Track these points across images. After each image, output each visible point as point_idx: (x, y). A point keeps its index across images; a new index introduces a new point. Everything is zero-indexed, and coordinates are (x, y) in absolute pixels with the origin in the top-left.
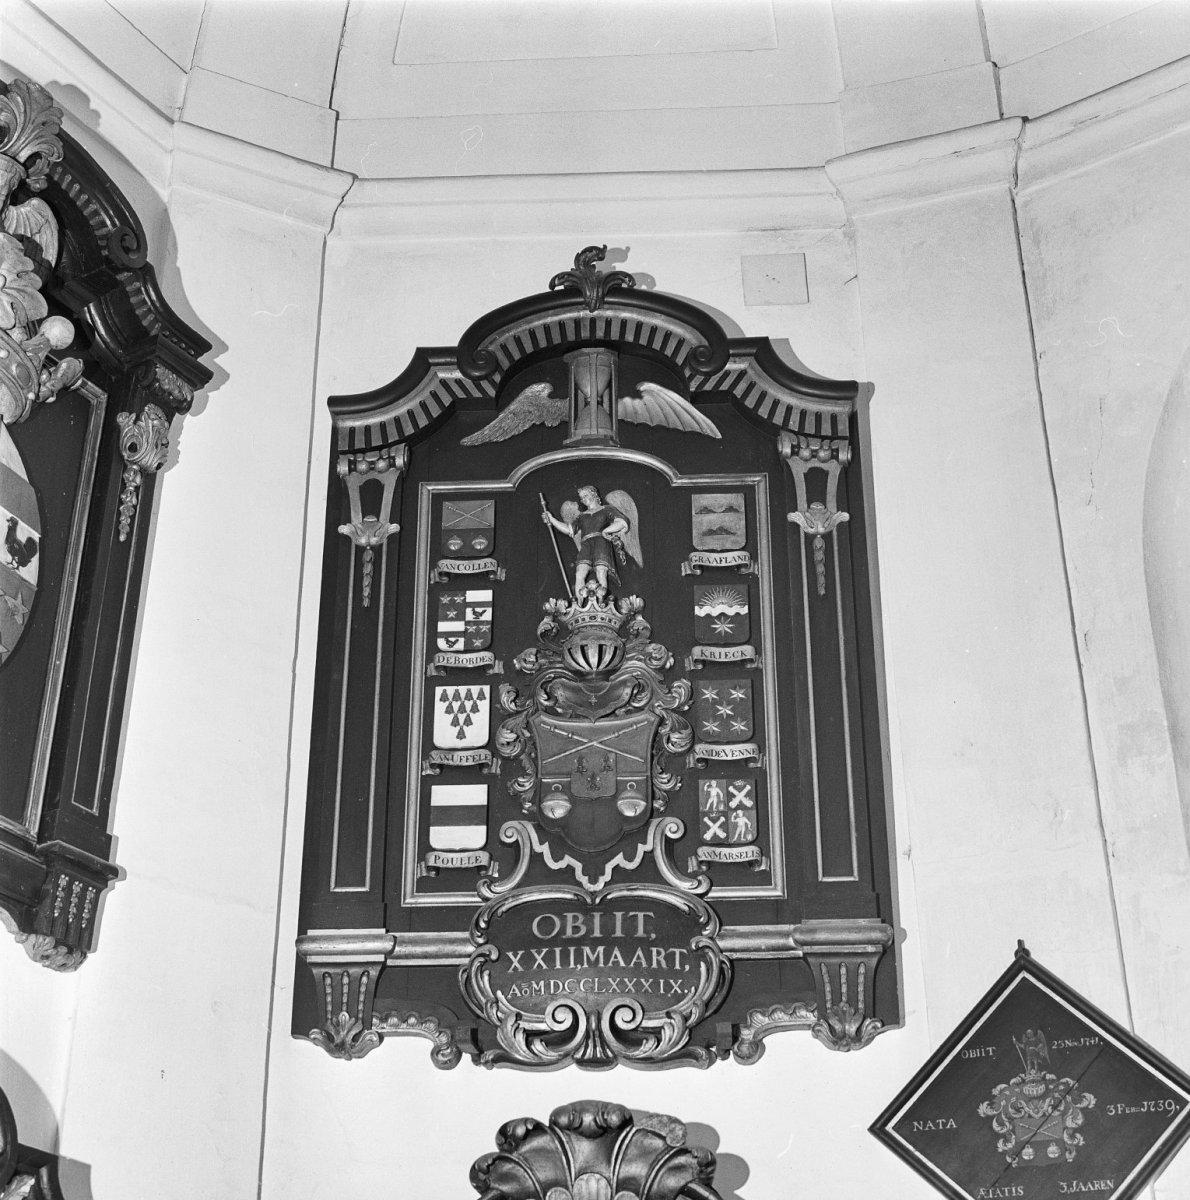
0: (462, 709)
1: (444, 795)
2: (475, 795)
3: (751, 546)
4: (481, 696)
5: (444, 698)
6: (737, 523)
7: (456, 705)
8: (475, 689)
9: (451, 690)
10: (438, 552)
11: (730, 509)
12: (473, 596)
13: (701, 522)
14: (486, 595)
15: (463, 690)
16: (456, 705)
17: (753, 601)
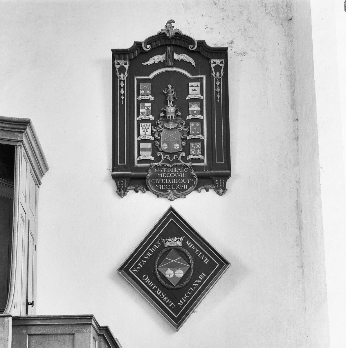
0: (145, 129)
1: (142, 145)
2: (149, 145)
3: (201, 93)
4: (149, 126)
5: (143, 129)
6: (198, 89)
7: (144, 128)
8: (148, 124)
9: (143, 124)
10: (139, 94)
11: (197, 86)
12: (147, 104)
13: (191, 89)
14: (149, 104)
15: (145, 124)
16: (144, 128)
17: (202, 107)
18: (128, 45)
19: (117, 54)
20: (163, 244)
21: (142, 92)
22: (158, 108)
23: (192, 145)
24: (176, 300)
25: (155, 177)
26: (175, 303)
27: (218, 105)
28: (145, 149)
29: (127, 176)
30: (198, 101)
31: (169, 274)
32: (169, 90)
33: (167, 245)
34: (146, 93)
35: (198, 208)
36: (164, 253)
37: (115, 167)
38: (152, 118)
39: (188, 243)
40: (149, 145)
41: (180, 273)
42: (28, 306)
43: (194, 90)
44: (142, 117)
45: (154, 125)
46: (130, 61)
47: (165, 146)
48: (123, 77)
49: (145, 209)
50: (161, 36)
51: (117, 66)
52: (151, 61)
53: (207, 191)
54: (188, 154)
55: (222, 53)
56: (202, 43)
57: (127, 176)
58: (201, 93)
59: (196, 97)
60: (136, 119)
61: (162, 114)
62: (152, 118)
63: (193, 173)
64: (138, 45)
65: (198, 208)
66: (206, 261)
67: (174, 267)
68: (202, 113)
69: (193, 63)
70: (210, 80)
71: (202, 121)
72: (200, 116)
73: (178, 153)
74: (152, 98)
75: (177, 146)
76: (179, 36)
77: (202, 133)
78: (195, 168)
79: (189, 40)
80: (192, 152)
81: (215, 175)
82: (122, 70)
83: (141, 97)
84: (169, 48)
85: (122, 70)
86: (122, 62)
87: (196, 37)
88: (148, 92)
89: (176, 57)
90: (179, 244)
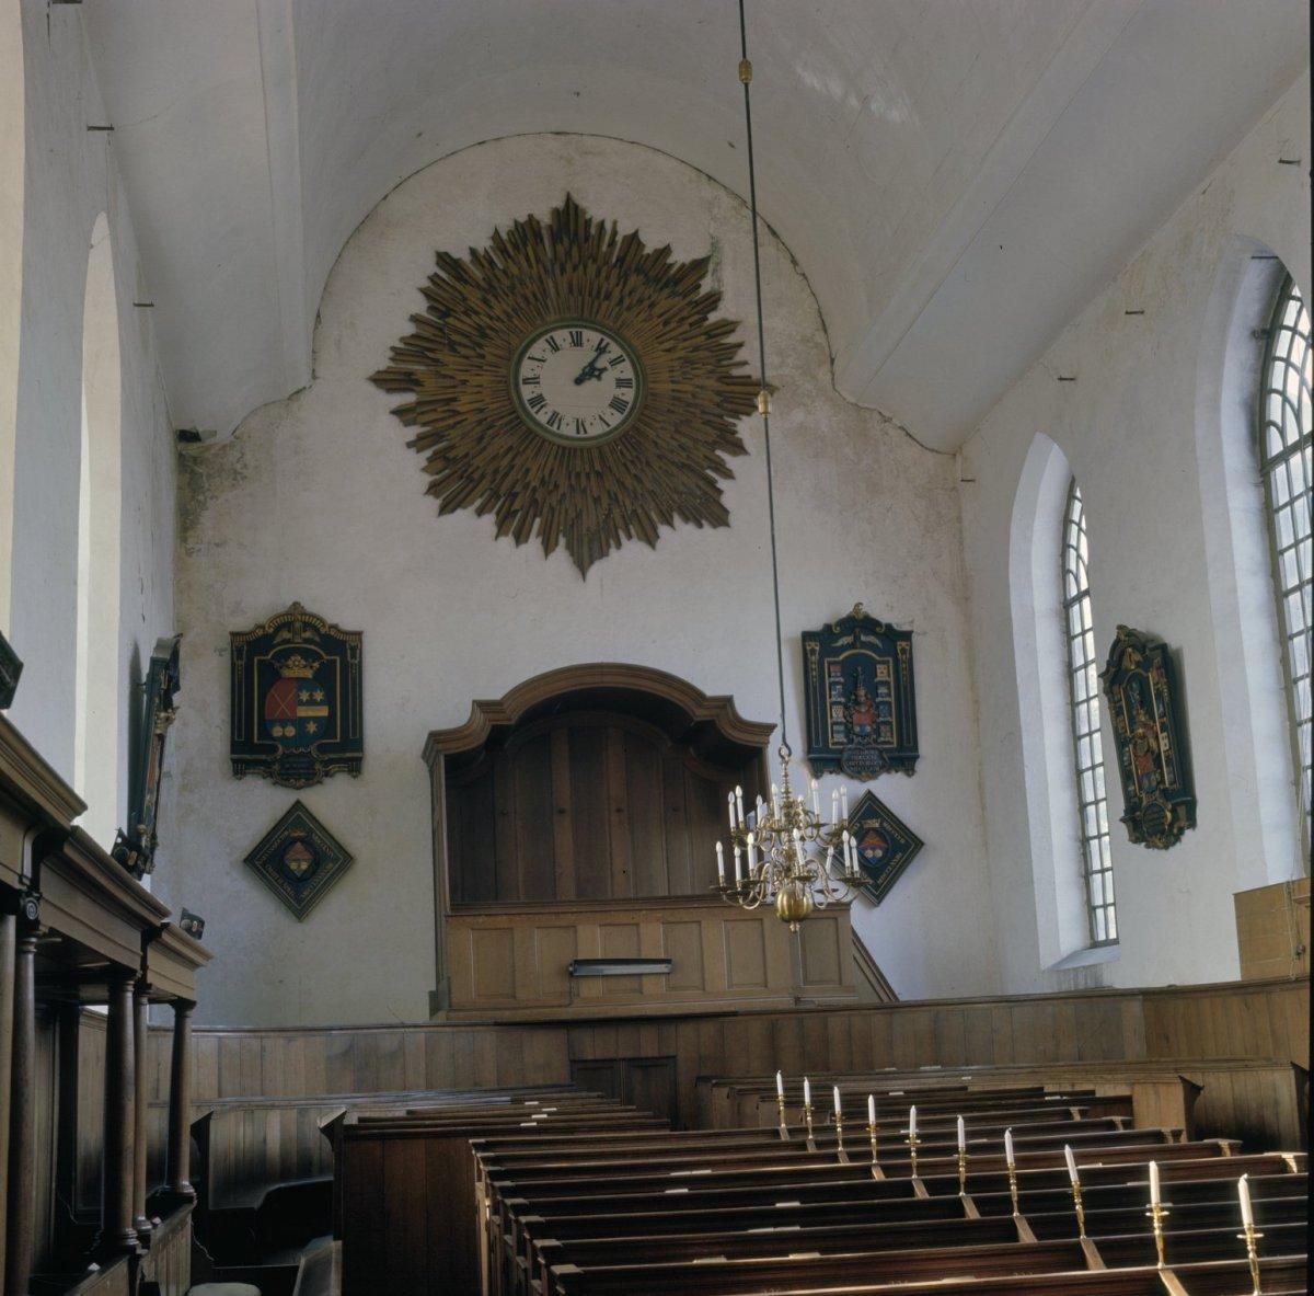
1: (835, 728)
3: (889, 676)
6: (885, 671)
10: (830, 676)
13: (878, 671)
19: (807, 636)
20: (862, 826)
21: (833, 674)
22: (850, 691)
23: (882, 728)
24: (875, 878)
25: (849, 760)
26: (877, 879)
27: (905, 688)
28: (838, 732)
30: (886, 684)
33: (867, 826)
38: (843, 700)
39: (885, 824)
40: (842, 728)
41: (879, 853)
42: (200, 943)
43: (883, 673)
44: (834, 699)
45: (846, 707)
46: (820, 647)
47: (857, 729)
51: (808, 648)
52: (840, 643)
53: (897, 771)
54: (879, 735)
55: (907, 636)
56: (889, 626)
58: (889, 676)
59: (884, 679)
60: (828, 701)
61: (853, 697)
62: (843, 700)
63: (885, 756)
64: (828, 627)
65: (890, 788)
66: (903, 841)
68: (889, 695)
69: (880, 645)
70: (896, 662)
71: (890, 703)
72: (887, 699)
73: (868, 735)
74: (842, 680)
75: (868, 729)
77: (891, 715)
78: (887, 750)
79: (877, 623)
80: (883, 734)
81: (903, 758)
82: (813, 651)
83: (832, 679)
84: (857, 630)
86: (813, 644)
88: (839, 674)
89: (863, 638)
90: (877, 825)
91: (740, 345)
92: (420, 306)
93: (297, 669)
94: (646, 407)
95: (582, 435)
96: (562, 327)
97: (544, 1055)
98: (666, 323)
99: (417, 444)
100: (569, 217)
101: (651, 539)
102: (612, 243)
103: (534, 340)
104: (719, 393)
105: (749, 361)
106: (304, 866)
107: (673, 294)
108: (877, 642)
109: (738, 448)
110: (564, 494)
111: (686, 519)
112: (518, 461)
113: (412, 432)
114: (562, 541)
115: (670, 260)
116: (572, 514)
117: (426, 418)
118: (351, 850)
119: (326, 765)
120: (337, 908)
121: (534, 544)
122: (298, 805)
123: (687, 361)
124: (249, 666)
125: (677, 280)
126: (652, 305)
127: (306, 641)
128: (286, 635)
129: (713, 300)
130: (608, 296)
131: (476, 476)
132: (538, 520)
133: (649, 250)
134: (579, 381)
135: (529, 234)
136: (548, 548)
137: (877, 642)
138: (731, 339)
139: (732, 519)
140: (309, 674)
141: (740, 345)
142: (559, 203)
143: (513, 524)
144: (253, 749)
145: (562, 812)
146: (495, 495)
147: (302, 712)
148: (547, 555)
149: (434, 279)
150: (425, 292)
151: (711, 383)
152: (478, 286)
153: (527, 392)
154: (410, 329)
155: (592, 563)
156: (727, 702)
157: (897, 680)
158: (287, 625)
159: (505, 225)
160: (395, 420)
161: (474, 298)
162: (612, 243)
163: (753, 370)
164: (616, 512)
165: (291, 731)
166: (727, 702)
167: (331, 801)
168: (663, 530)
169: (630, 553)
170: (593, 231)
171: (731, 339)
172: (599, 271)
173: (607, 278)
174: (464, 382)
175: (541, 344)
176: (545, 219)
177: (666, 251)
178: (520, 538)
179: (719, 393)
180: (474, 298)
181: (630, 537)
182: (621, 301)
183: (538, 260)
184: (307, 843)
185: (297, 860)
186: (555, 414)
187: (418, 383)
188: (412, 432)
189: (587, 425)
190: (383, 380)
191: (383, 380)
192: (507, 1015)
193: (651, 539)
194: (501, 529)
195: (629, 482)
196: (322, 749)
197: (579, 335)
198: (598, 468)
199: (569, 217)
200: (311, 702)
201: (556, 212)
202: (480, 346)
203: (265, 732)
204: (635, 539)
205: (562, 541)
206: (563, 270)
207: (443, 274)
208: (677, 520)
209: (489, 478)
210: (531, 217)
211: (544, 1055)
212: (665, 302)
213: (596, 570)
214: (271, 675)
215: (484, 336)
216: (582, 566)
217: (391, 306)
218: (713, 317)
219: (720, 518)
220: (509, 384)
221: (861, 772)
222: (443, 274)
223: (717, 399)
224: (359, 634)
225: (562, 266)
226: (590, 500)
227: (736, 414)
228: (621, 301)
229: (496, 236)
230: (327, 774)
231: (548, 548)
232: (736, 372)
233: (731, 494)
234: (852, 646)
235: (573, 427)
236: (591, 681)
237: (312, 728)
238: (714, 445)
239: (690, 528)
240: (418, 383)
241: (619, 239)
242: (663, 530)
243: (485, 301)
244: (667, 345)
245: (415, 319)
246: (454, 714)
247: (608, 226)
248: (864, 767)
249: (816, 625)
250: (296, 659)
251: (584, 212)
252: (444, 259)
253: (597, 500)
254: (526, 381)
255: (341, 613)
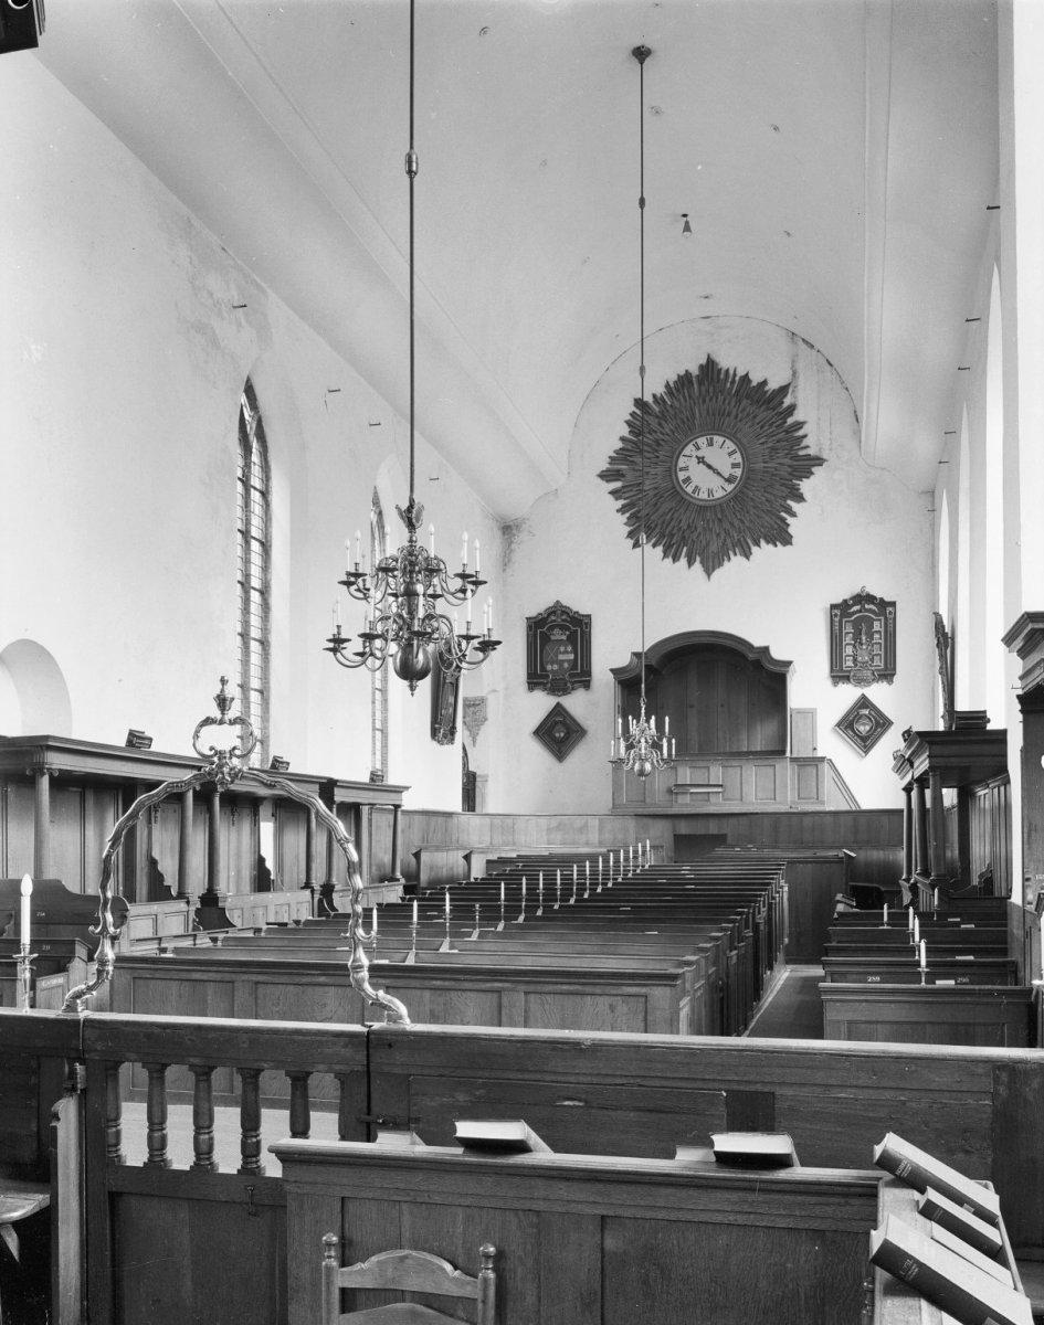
18: (839, 601)
19: (833, 607)
29: (839, 675)
31: (862, 728)
32: (862, 628)
34: (849, 628)
35: (878, 693)
36: (859, 717)
37: (832, 670)
41: (868, 728)
43: (877, 626)
45: (854, 646)
46: (840, 611)
48: (837, 619)
49: (848, 694)
50: (858, 596)
55: (893, 604)
56: (881, 599)
57: (839, 675)
64: (845, 601)
65: (878, 693)
67: (864, 724)
70: (886, 619)
76: (868, 595)
79: (875, 598)
81: (887, 674)
82: (836, 615)
85: (836, 615)
87: (878, 596)
89: (866, 606)
91: (805, 436)
92: (625, 431)
93: (558, 635)
94: (749, 478)
95: (711, 498)
96: (702, 436)
97: (661, 830)
98: (762, 427)
99: (622, 510)
100: (710, 367)
101: (747, 554)
102: (733, 382)
103: (686, 445)
104: (789, 466)
105: (812, 445)
106: (562, 735)
107: (768, 409)
108: (874, 608)
109: (800, 498)
110: (700, 534)
111: (768, 542)
112: (676, 515)
113: (620, 503)
114: (698, 559)
115: (767, 388)
116: (704, 542)
117: (627, 495)
118: (585, 728)
119: (573, 683)
120: (578, 756)
121: (683, 561)
122: (558, 705)
123: (772, 449)
124: (535, 635)
125: (770, 400)
126: (755, 417)
127: (563, 620)
128: (553, 618)
129: (792, 409)
130: (729, 415)
131: (653, 525)
132: (685, 549)
133: (754, 384)
134: (486, 582)
135: (686, 382)
136: (690, 563)
137: (874, 608)
138: (801, 433)
139: (794, 540)
140: (564, 638)
141: (805, 436)
142: (704, 361)
143: (671, 552)
144: (536, 679)
145: (692, 706)
146: (662, 536)
147: (561, 657)
148: (689, 566)
149: (633, 414)
150: (627, 422)
151: (787, 461)
152: (657, 417)
153: (682, 476)
154: (620, 445)
155: (713, 570)
156: (766, 649)
157: (886, 631)
158: (554, 612)
159: (673, 378)
160: (611, 497)
161: (653, 422)
162: (733, 382)
163: (812, 452)
164: (729, 541)
165: (556, 667)
166: (766, 649)
167: (576, 703)
168: (754, 549)
169: (736, 562)
170: (722, 376)
171: (801, 433)
172: (725, 400)
173: (729, 404)
174: (647, 473)
175: (690, 446)
176: (695, 371)
177: (765, 383)
178: (676, 559)
179: (789, 466)
180: (653, 422)
181: (735, 554)
182: (736, 417)
183: (690, 397)
184: (564, 723)
185: (559, 732)
186: (696, 487)
187: (623, 476)
188: (620, 503)
189: (714, 493)
190: (606, 476)
191: (606, 476)
192: (640, 811)
193: (747, 554)
194: (665, 555)
195: (736, 523)
196: (571, 676)
197: (712, 439)
198: (719, 516)
199: (710, 367)
200: (566, 652)
201: (701, 367)
202: (656, 451)
203: (543, 668)
204: (739, 556)
205: (698, 559)
206: (704, 401)
207: (638, 412)
208: (763, 543)
209: (659, 527)
210: (687, 371)
211: (661, 830)
212: (763, 414)
213: (717, 574)
214: (546, 639)
215: (658, 445)
216: (709, 572)
217: (610, 433)
218: (790, 421)
219: (786, 540)
220: (671, 471)
221: (860, 682)
222: (638, 412)
223: (789, 470)
224: (589, 616)
225: (710, 399)
226: (715, 538)
227: (800, 478)
228: (736, 417)
229: (667, 385)
230: (573, 689)
231: (690, 563)
232: (801, 453)
233: (794, 526)
234: (860, 611)
235: (706, 493)
236: (696, 640)
237: (566, 665)
238: (785, 498)
239: (771, 546)
240: (623, 476)
241: (737, 378)
242: (754, 549)
243: (660, 424)
244: (763, 440)
245: (623, 439)
246: (623, 660)
247: (731, 372)
248: (863, 680)
249: (839, 600)
250: (556, 631)
251: (717, 364)
252: (639, 403)
253: (718, 535)
254: (681, 470)
255: (579, 606)
